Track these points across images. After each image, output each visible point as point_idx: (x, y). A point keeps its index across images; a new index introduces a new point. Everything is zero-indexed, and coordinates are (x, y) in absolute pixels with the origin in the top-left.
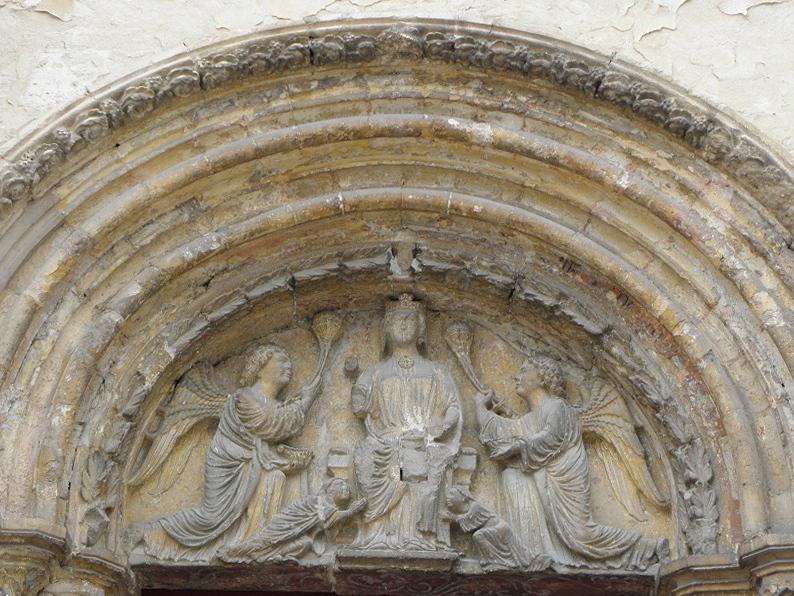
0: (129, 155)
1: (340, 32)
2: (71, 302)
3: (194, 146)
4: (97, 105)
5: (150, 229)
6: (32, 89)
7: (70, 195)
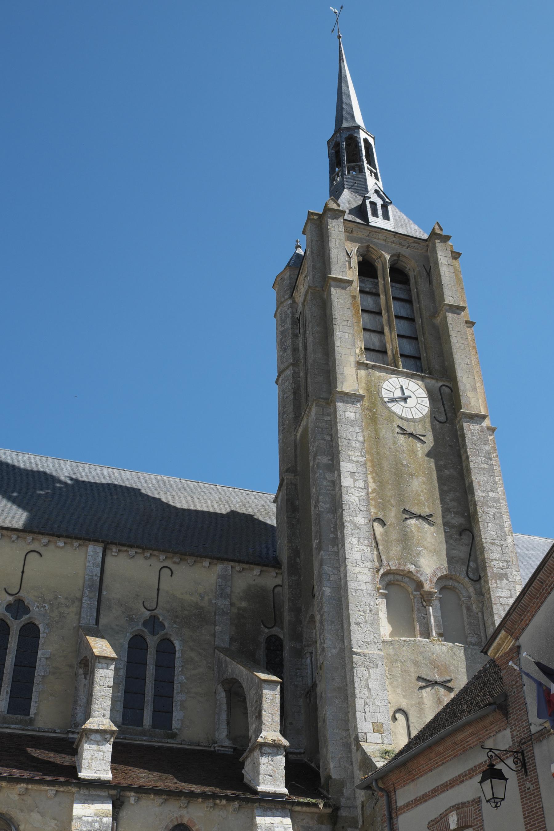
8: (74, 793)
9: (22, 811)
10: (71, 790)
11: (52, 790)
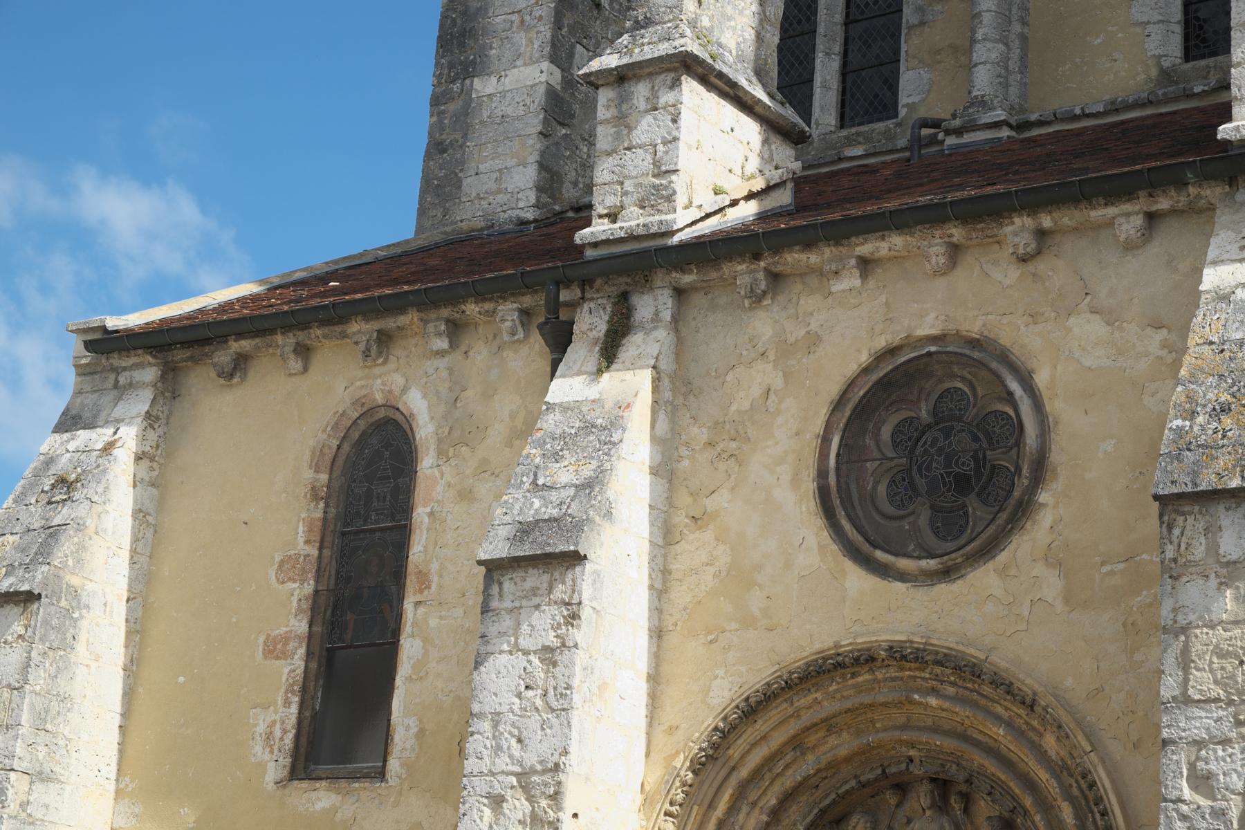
0: (761, 725)
1: (851, 651)
2: (745, 809)
3: (796, 715)
4: (737, 707)
5: (782, 762)
6: (711, 694)
7: (735, 752)
8: (1211, 208)
9: (1034, 317)
10: (1198, 196)
11: (1128, 215)
